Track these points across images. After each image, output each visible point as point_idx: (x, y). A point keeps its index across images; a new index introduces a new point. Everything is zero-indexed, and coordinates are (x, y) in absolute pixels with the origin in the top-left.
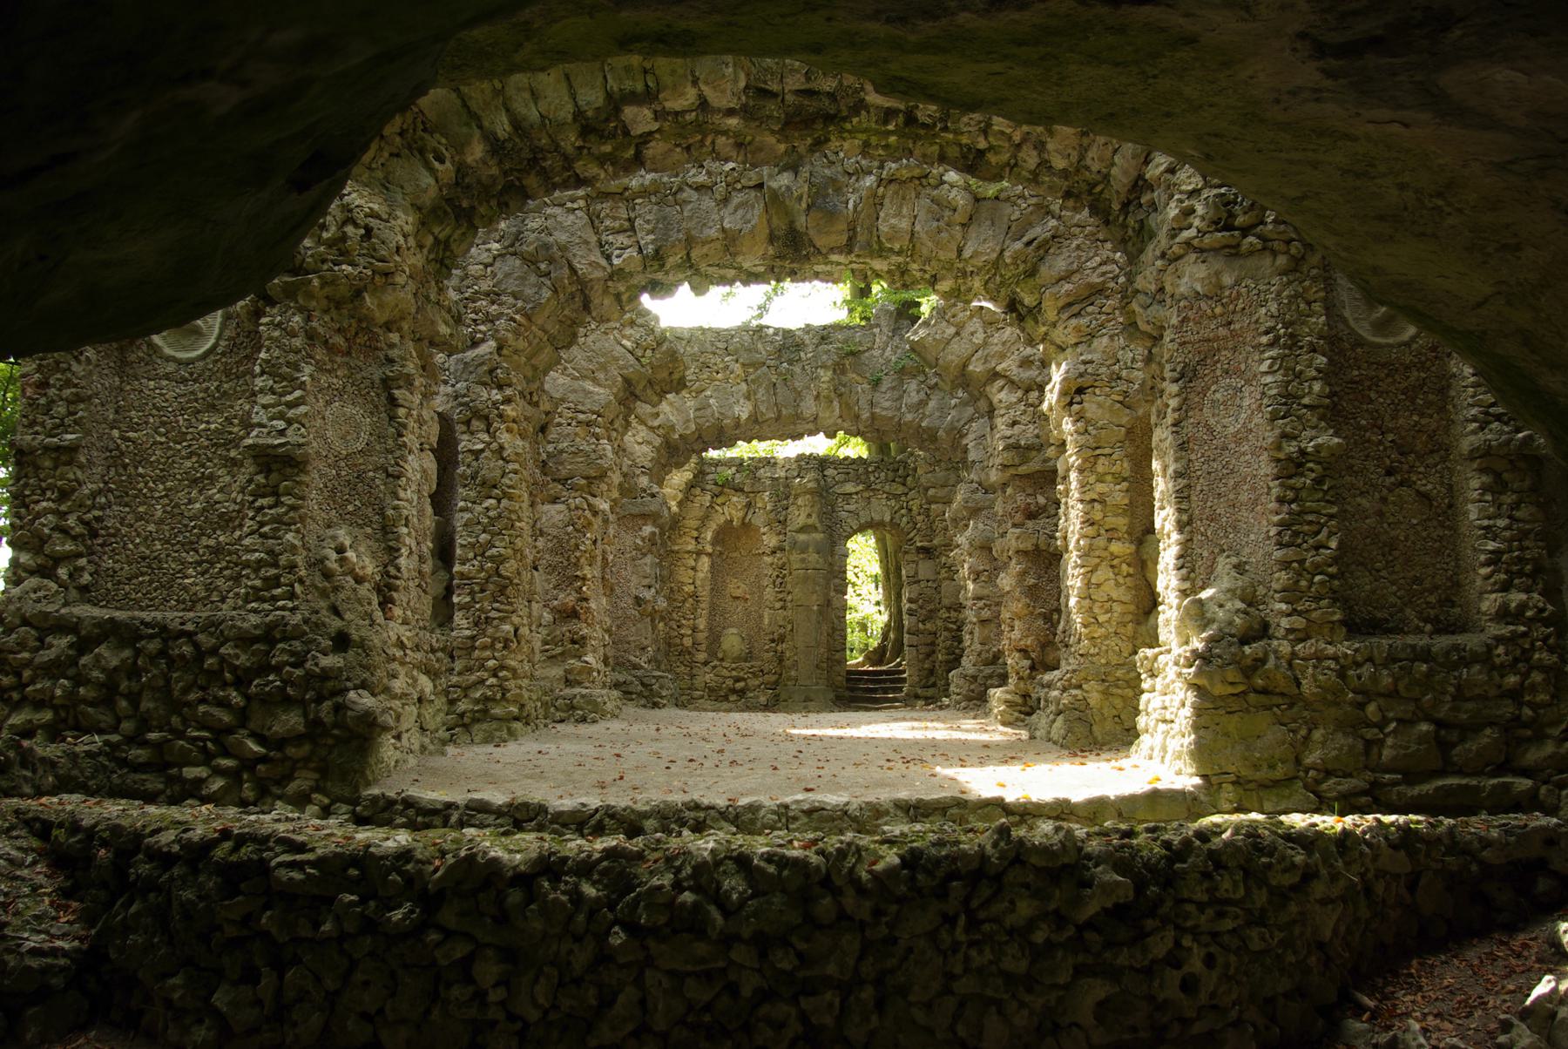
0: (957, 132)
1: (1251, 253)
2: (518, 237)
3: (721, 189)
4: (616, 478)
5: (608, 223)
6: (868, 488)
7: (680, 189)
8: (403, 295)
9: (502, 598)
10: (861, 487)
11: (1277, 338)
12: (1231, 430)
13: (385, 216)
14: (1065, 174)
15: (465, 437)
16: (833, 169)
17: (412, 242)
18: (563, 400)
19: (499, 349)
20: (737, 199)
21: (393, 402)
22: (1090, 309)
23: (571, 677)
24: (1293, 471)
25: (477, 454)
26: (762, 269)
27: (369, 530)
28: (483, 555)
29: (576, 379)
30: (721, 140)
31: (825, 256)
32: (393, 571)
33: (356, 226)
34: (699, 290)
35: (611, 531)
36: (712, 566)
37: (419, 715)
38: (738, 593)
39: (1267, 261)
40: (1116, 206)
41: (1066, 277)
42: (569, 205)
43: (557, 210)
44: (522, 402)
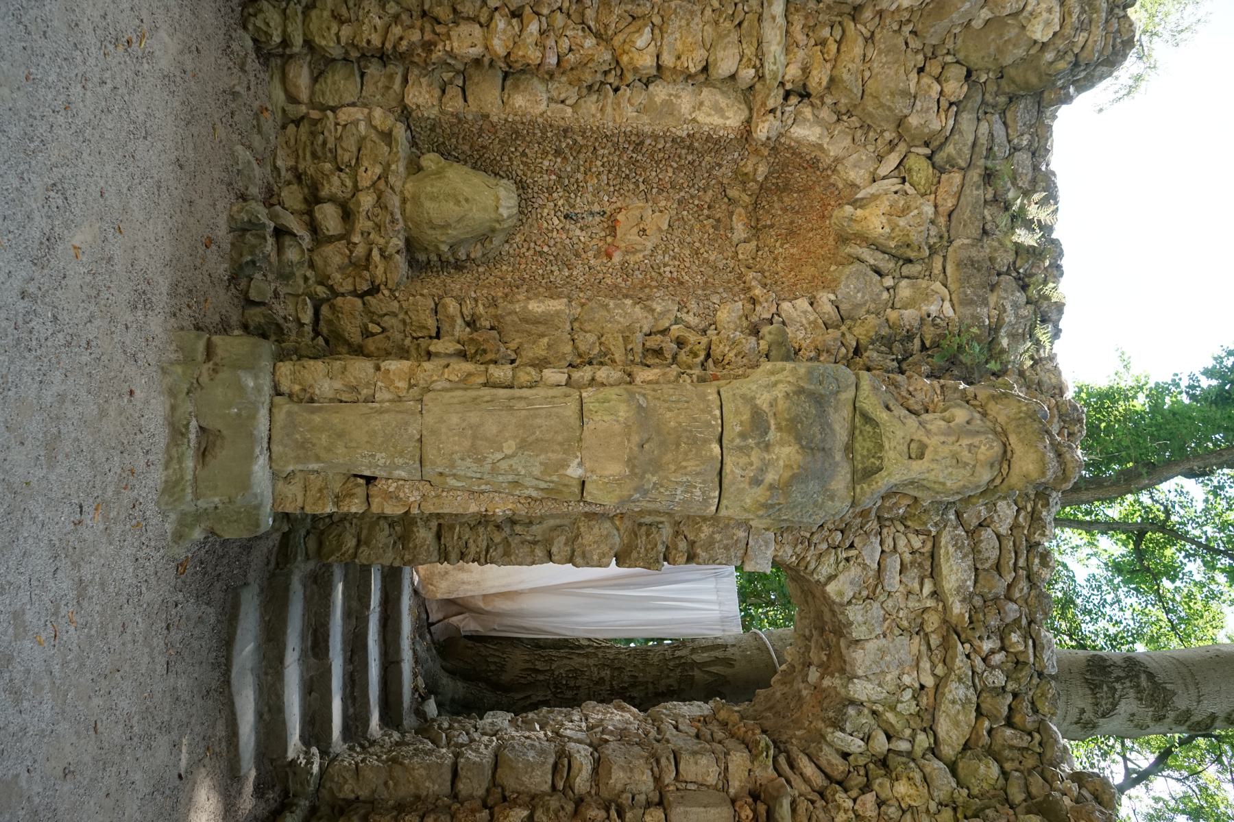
6: (951, 630)
10: (958, 608)
36: (715, 144)
38: (628, 235)
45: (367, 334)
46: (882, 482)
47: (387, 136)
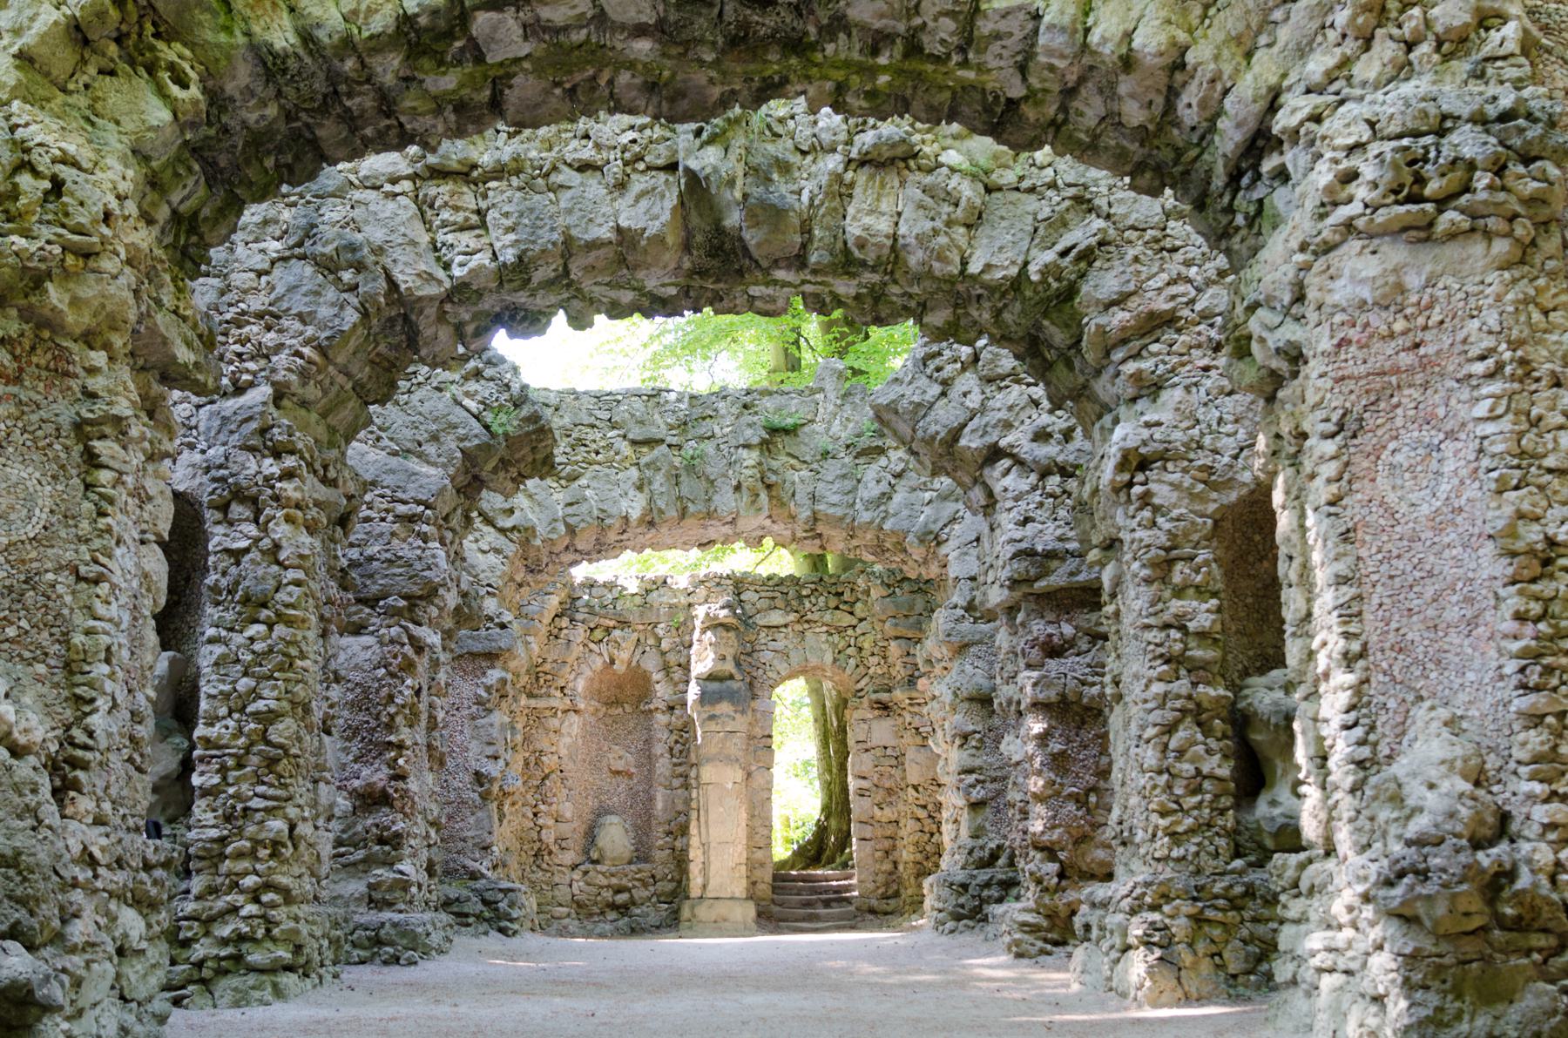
0: (981, 68)
1: (1453, 235)
2: (310, 231)
3: (616, 168)
4: (451, 599)
5: (446, 215)
7: (555, 168)
8: (114, 285)
9: (271, 778)
11: (1500, 367)
12: (1425, 509)
13: (85, 165)
14: (1143, 134)
15: (220, 529)
16: (780, 143)
17: (131, 208)
18: (374, 484)
19: (278, 398)
20: (639, 183)
21: (92, 460)
22: (1154, 348)
23: (377, 895)
24: (1539, 570)
25: (237, 555)
26: (673, 291)
27: (41, 668)
28: (242, 710)
29: (395, 454)
30: (624, 78)
31: (766, 272)
32: (79, 735)
33: (36, 174)
34: (579, 321)
35: (442, 677)
37: (118, 976)
38: (620, 765)
39: (1477, 248)
40: (1219, 181)
41: (1120, 301)
42: (388, 187)
43: (371, 195)
44: (311, 479)
45: (672, 880)
46: (734, 671)
47: (586, 873)
